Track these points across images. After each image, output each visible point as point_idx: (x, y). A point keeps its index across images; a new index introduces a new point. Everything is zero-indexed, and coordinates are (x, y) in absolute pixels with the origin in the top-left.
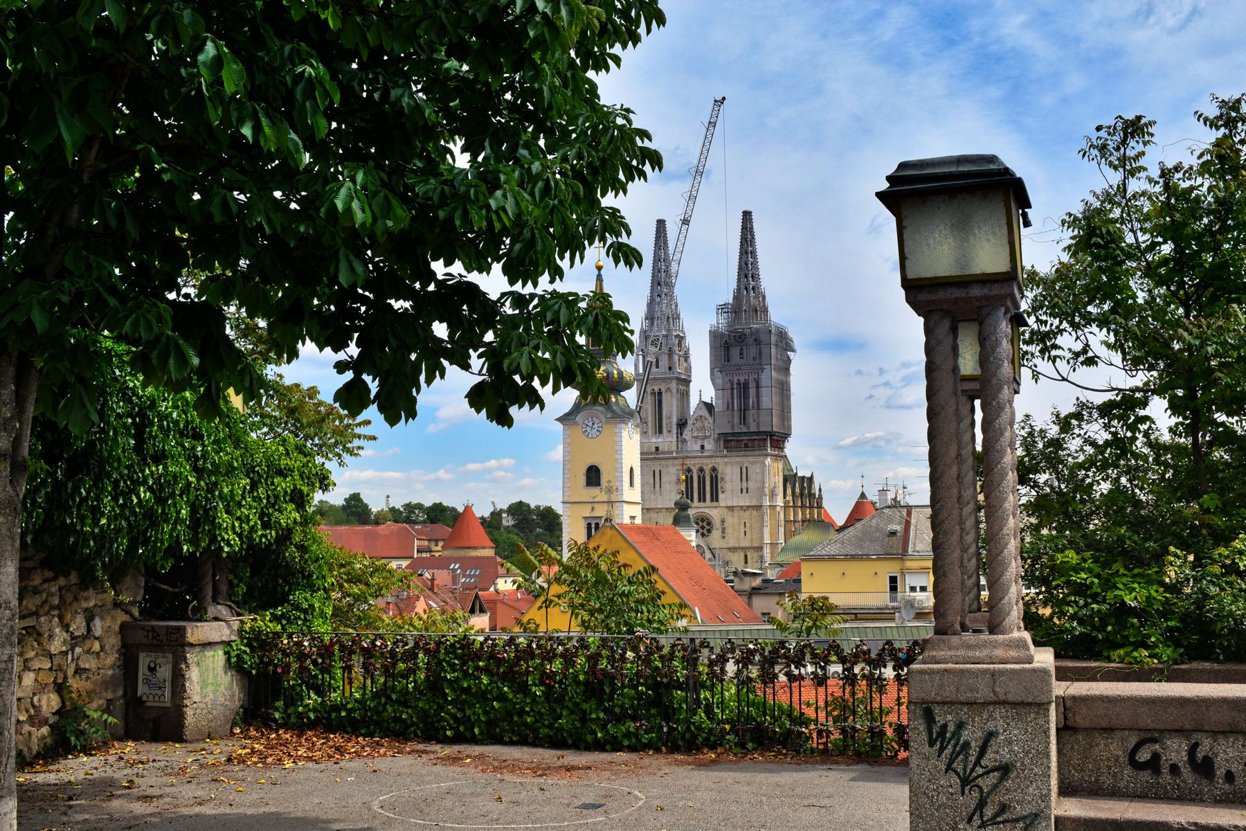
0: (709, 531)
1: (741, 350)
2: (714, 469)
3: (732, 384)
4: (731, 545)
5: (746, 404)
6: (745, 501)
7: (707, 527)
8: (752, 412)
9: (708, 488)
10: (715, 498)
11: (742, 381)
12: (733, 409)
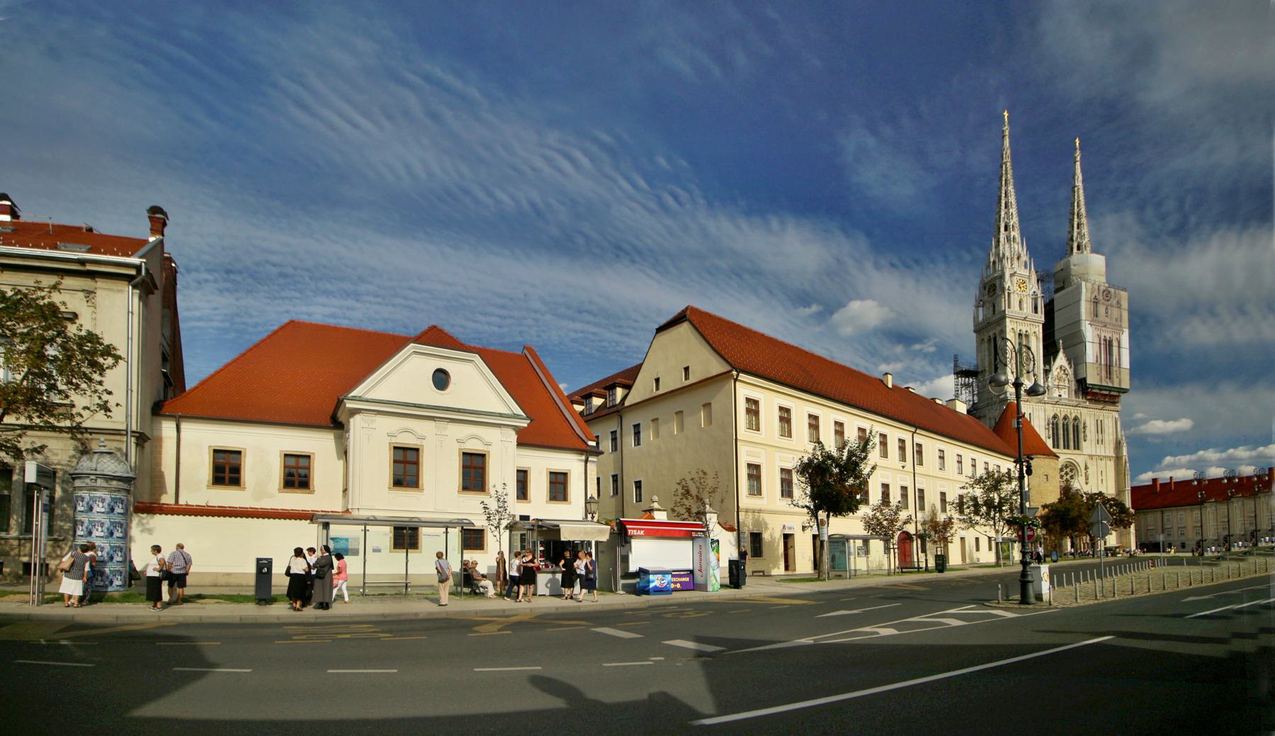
1: (1107, 309)
2: (1076, 419)
5: (1111, 360)
6: (1100, 451)
9: (1061, 436)
10: (1077, 447)
11: (1108, 339)
12: (1101, 364)
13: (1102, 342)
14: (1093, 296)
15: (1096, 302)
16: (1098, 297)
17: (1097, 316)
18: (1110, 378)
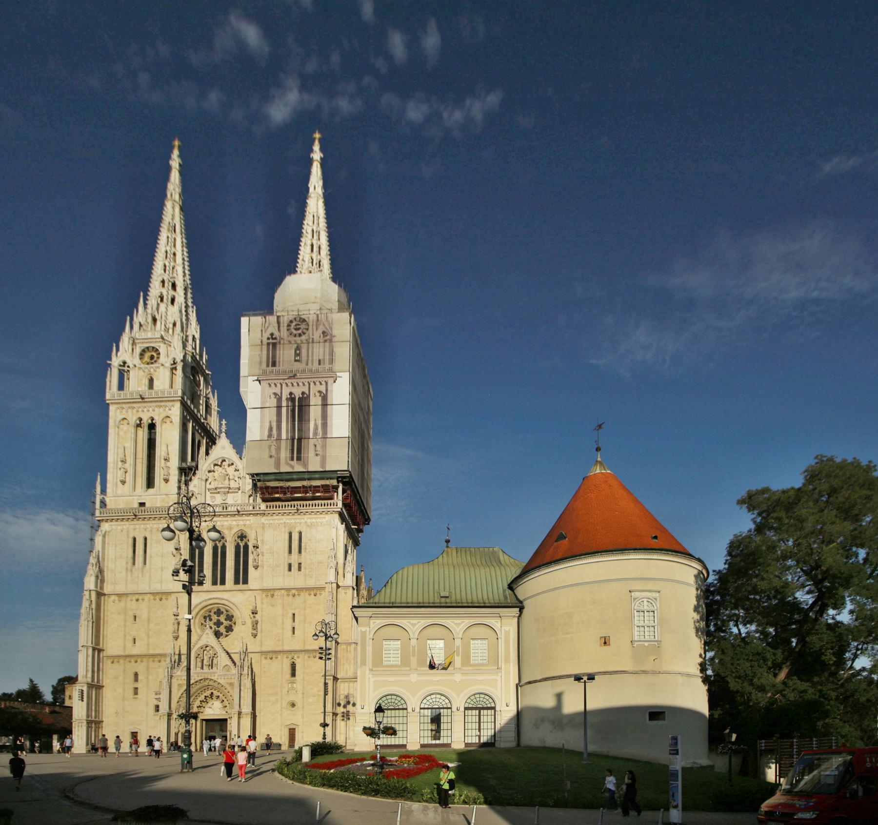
0: (229, 629)
1: (298, 348)
3: (279, 400)
4: (264, 649)
7: (226, 623)
8: (312, 442)
10: (241, 577)
12: (279, 439)
13: (284, 404)
14: (267, 335)
15: (273, 344)
16: (277, 334)
17: (274, 364)
18: (299, 459)
